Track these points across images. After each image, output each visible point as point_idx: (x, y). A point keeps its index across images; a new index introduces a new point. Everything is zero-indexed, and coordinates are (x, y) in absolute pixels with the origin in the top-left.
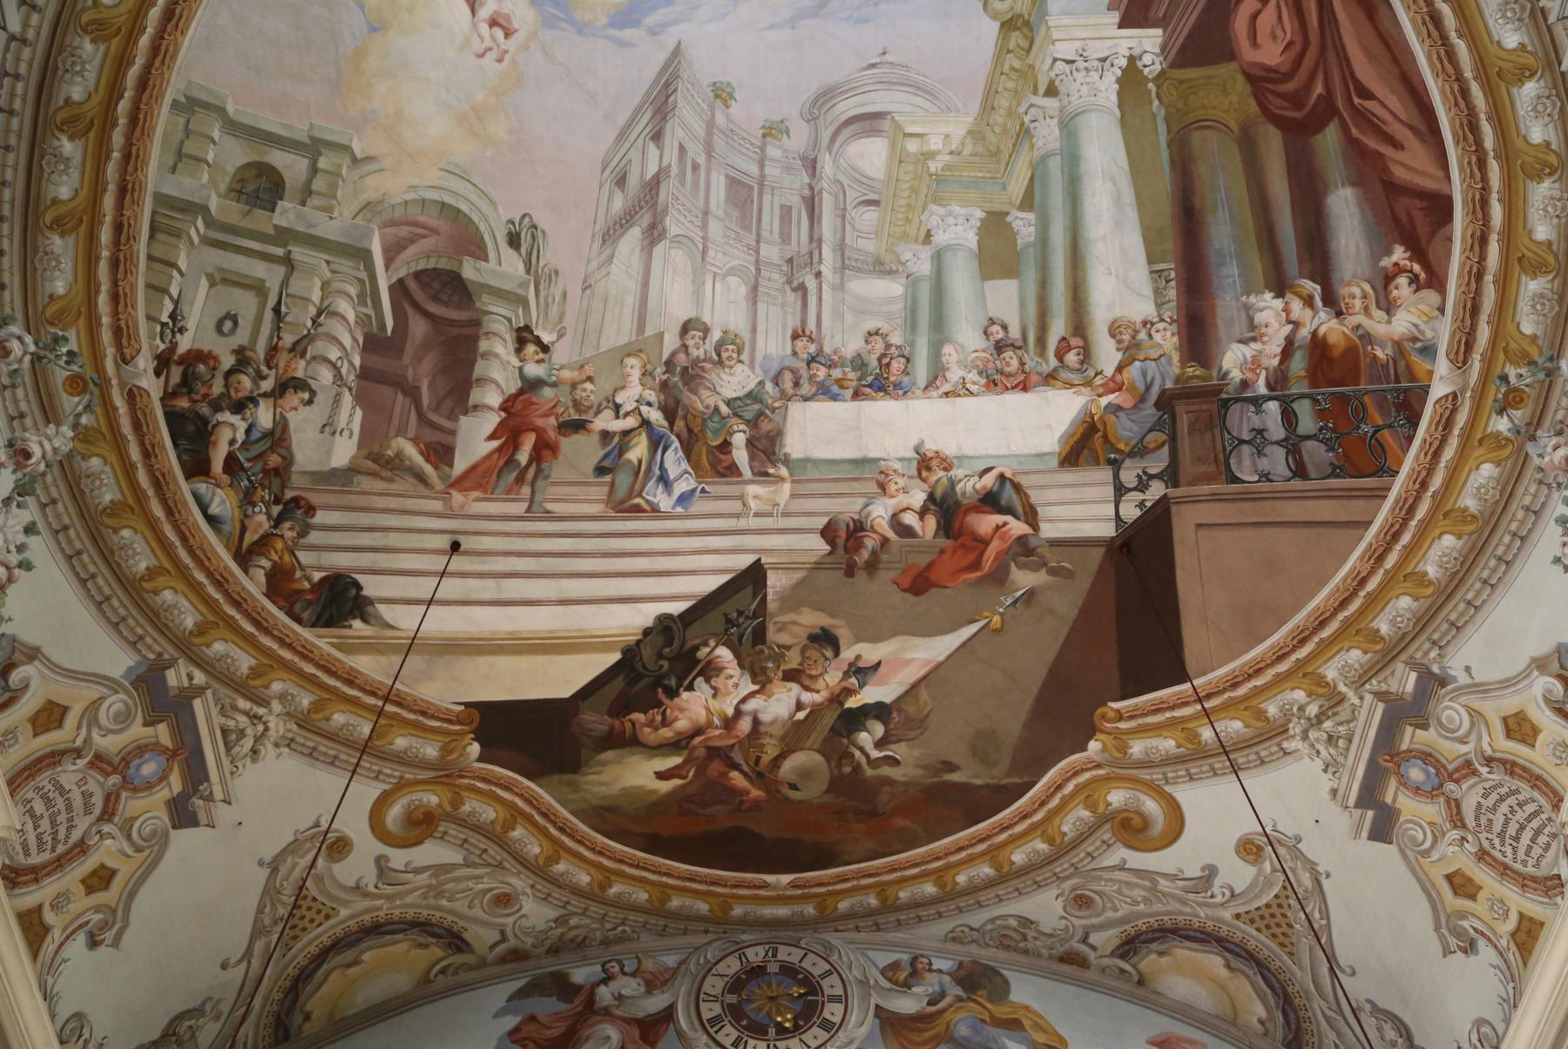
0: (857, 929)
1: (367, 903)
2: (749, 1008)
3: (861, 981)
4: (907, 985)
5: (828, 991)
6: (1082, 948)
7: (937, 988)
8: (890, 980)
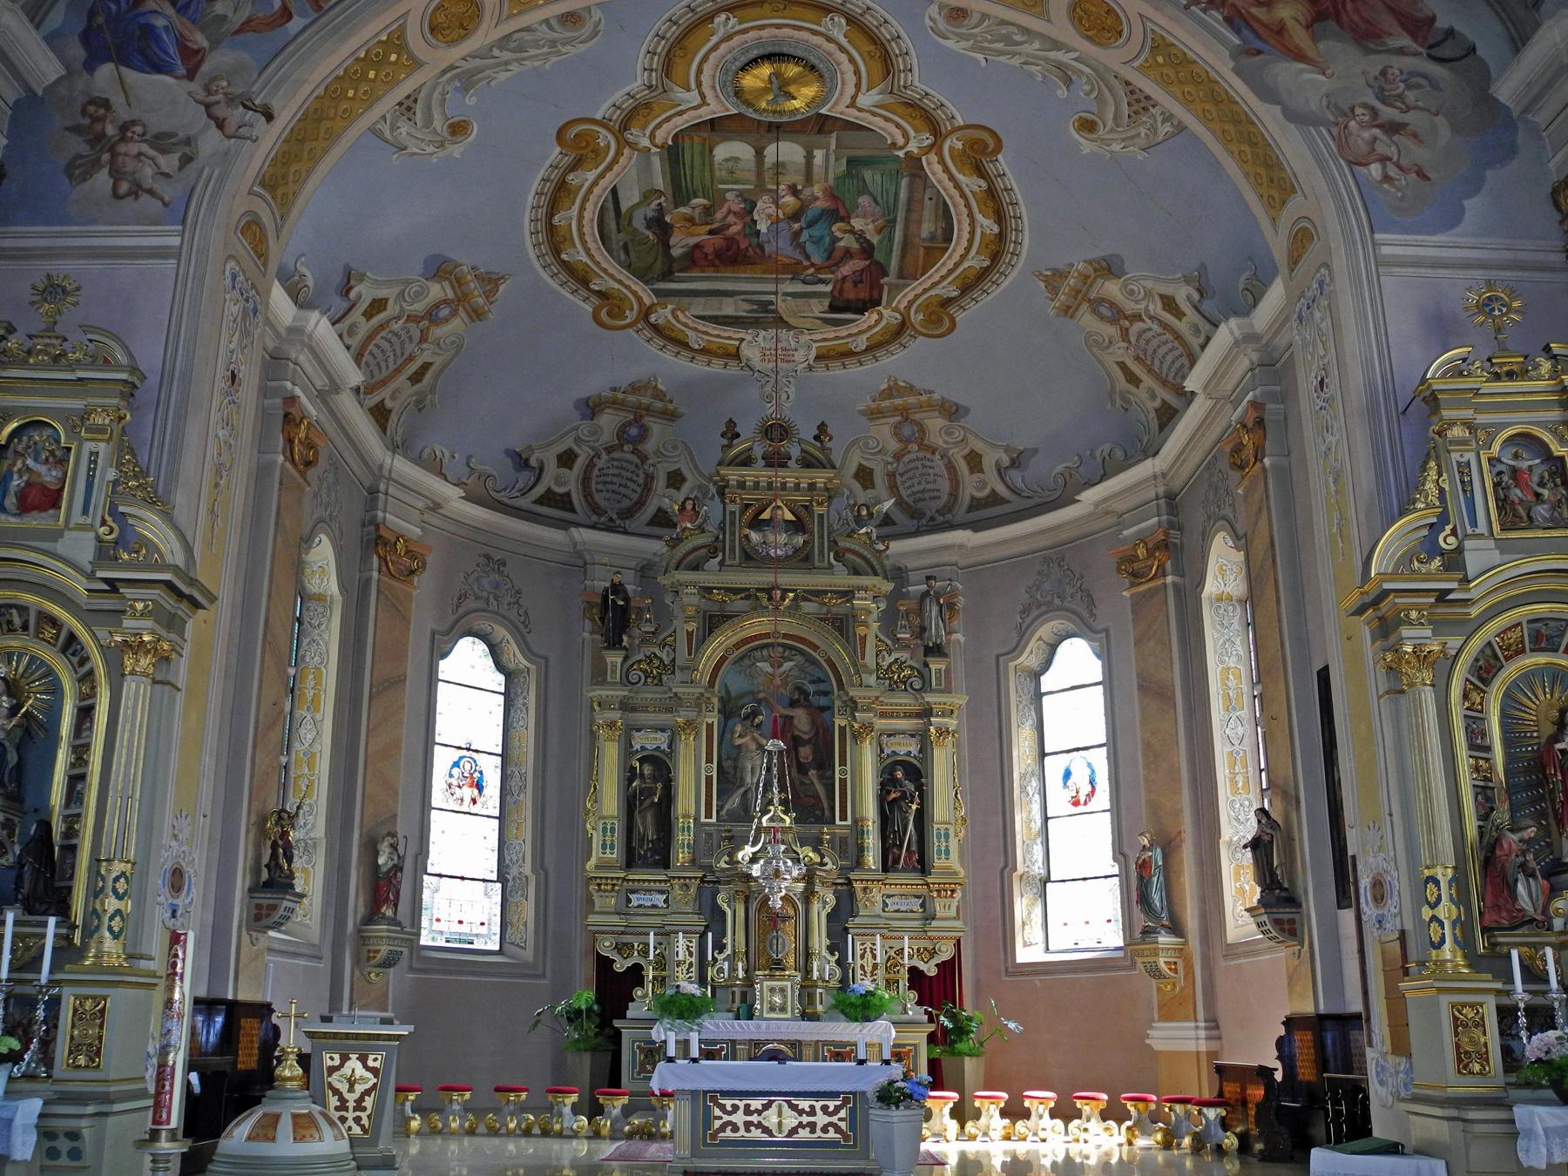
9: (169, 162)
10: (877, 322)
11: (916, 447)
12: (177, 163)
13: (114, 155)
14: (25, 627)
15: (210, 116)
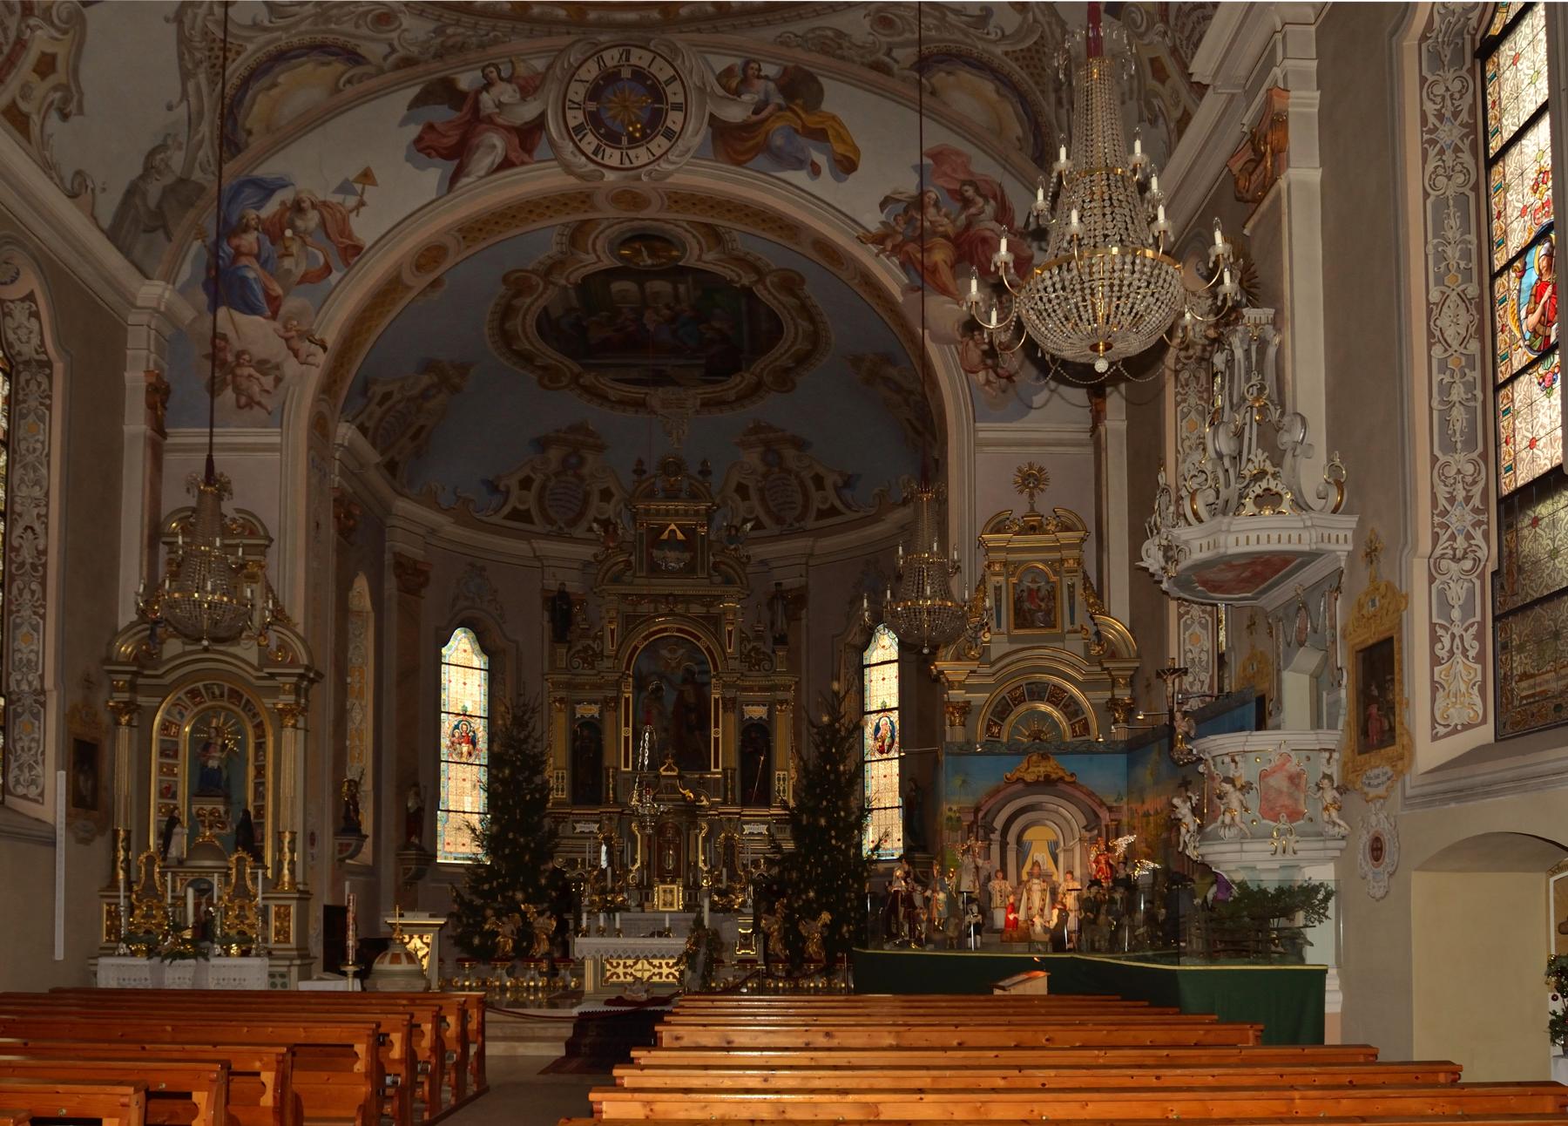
0: (699, 31)
1: (268, 36)
2: (606, 115)
3: (699, 88)
4: (737, 93)
5: (672, 99)
6: (887, 59)
7: (762, 96)
8: (724, 87)
9: (268, 381)
10: (741, 382)
11: (776, 470)
12: (272, 383)
13: (235, 376)
14: (222, 695)
15: (290, 348)
